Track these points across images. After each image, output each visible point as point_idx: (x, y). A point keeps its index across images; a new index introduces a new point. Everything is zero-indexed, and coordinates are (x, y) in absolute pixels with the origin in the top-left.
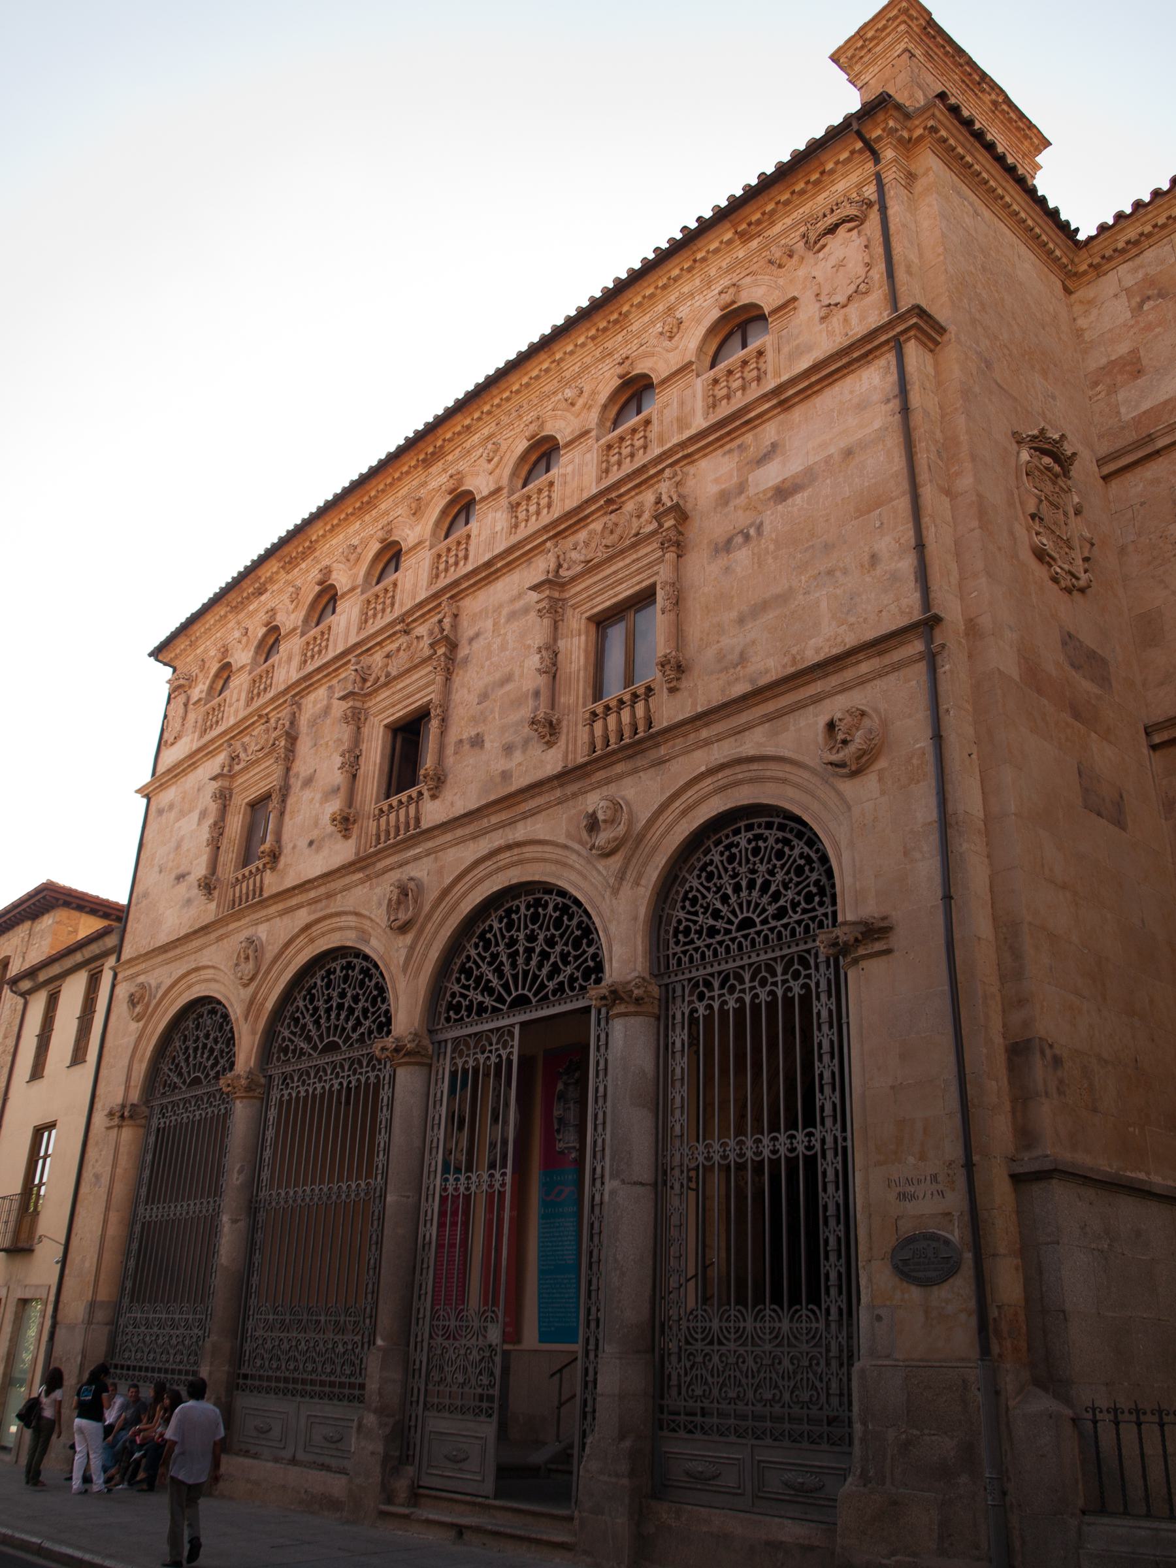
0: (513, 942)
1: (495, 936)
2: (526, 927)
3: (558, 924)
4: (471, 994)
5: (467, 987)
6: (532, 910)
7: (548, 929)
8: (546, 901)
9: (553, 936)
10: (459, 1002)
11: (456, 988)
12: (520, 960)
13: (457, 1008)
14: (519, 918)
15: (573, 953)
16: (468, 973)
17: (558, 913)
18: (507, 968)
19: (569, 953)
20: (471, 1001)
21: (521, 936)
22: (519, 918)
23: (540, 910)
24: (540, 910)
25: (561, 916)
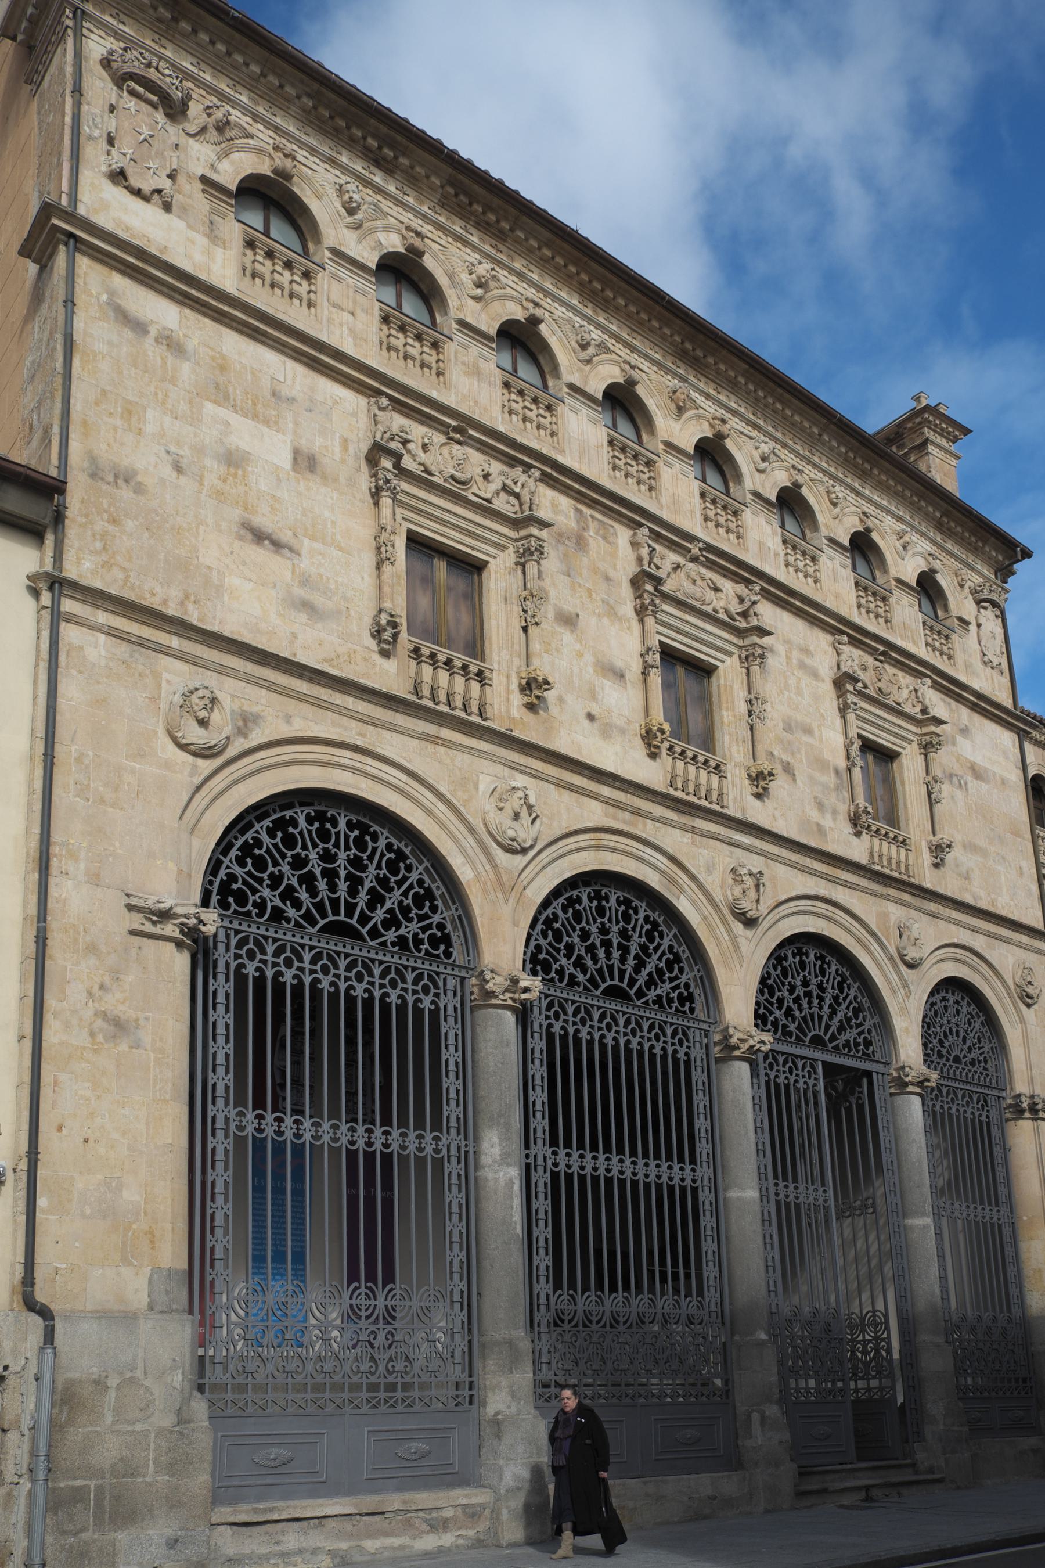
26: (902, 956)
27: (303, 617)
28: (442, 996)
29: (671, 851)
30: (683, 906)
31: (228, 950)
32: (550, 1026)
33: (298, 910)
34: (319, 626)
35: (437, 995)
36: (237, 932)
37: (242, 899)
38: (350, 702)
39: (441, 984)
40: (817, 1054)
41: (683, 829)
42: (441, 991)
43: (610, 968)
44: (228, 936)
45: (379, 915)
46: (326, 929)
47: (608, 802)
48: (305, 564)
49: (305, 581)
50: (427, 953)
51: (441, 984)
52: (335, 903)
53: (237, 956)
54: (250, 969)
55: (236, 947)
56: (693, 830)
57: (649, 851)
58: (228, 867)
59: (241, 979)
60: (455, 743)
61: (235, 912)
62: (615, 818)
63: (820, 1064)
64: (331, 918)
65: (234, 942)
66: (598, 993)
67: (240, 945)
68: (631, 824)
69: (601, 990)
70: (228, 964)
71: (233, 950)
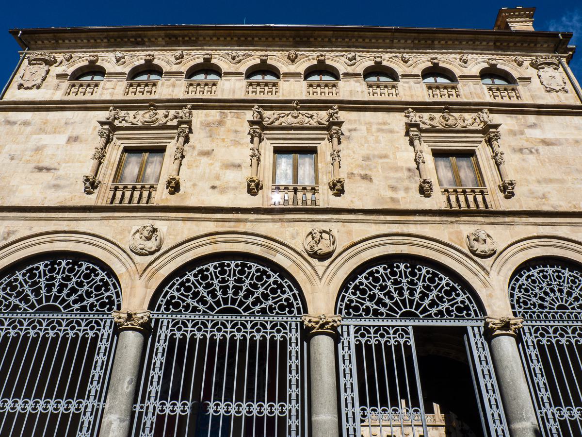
0: (68, 279)
1: (60, 269)
2: (79, 277)
3: (98, 288)
4: (26, 287)
5: (26, 282)
6: (88, 271)
7: (91, 287)
8: (98, 273)
9: (92, 292)
10: (16, 286)
11: (20, 278)
12: (66, 291)
13: (13, 288)
14: (78, 271)
15: (98, 307)
16: (33, 276)
17: (101, 284)
18: (55, 290)
19: (96, 306)
20: (23, 290)
21: (74, 280)
22: (78, 271)
23: (93, 275)
24: (93, 275)
25: (102, 286)
26: (474, 252)
27: (53, 190)
28: (102, 329)
29: (264, 234)
30: (279, 259)
31: (531, 335)
32: (539, 341)
33: (385, 307)
34: (60, 191)
35: (99, 330)
36: (533, 326)
37: (356, 309)
38: (66, 215)
39: (102, 324)
40: (410, 323)
41: (274, 221)
42: (102, 327)
43: (396, 304)
44: (529, 329)
45: (426, 302)
46: (403, 315)
47: (217, 220)
48: (61, 172)
49: (58, 178)
50: (456, 316)
51: (102, 324)
52: (411, 302)
53: (536, 337)
54: (544, 341)
55: (534, 333)
56: (281, 221)
57: (217, 236)
58: (348, 297)
59: (541, 348)
60: (119, 217)
61: (172, 311)
62: (222, 226)
63: (411, 329)
64: (404, 310)
65: (533, 331)
66: (398, 316)
67: (536, 332)
68: (234, 227)
69: (399, 314)
70: (533, 342)
71: (533, 335)
